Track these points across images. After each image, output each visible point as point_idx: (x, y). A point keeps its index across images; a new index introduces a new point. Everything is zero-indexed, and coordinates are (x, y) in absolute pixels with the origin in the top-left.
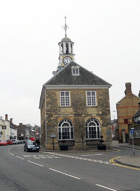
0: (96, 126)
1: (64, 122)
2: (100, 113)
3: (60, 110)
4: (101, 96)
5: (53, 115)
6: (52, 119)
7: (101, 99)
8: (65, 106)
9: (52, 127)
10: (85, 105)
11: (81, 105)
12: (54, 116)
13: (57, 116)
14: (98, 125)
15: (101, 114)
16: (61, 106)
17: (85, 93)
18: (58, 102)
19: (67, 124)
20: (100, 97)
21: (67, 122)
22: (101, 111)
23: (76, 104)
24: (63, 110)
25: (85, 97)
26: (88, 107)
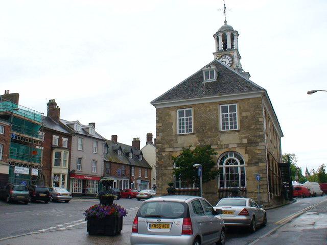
0: (239, 165)
1: (229, 157)
2: (245, 141)
3: (176, 140)
4: (246, 111)
5: (165, 148)
6: (164, 155)
7: (247, 117)
8: (185, 133)
9: (163, 168)
10: (217, 129)
11: (210, 130)
12: (167, 150)
13: (171, 150)
14: (242, 162)
15: (246, 144)
16: (178, 133)
17: (217, 110)
18: (173, 127)
19: (234, 161)
20: (244, 114)
21: (233, 157)
22: (245, 138)
23: (202, 129)
24: (180, 140)
25: (217, 116)
26: (222, 133)
